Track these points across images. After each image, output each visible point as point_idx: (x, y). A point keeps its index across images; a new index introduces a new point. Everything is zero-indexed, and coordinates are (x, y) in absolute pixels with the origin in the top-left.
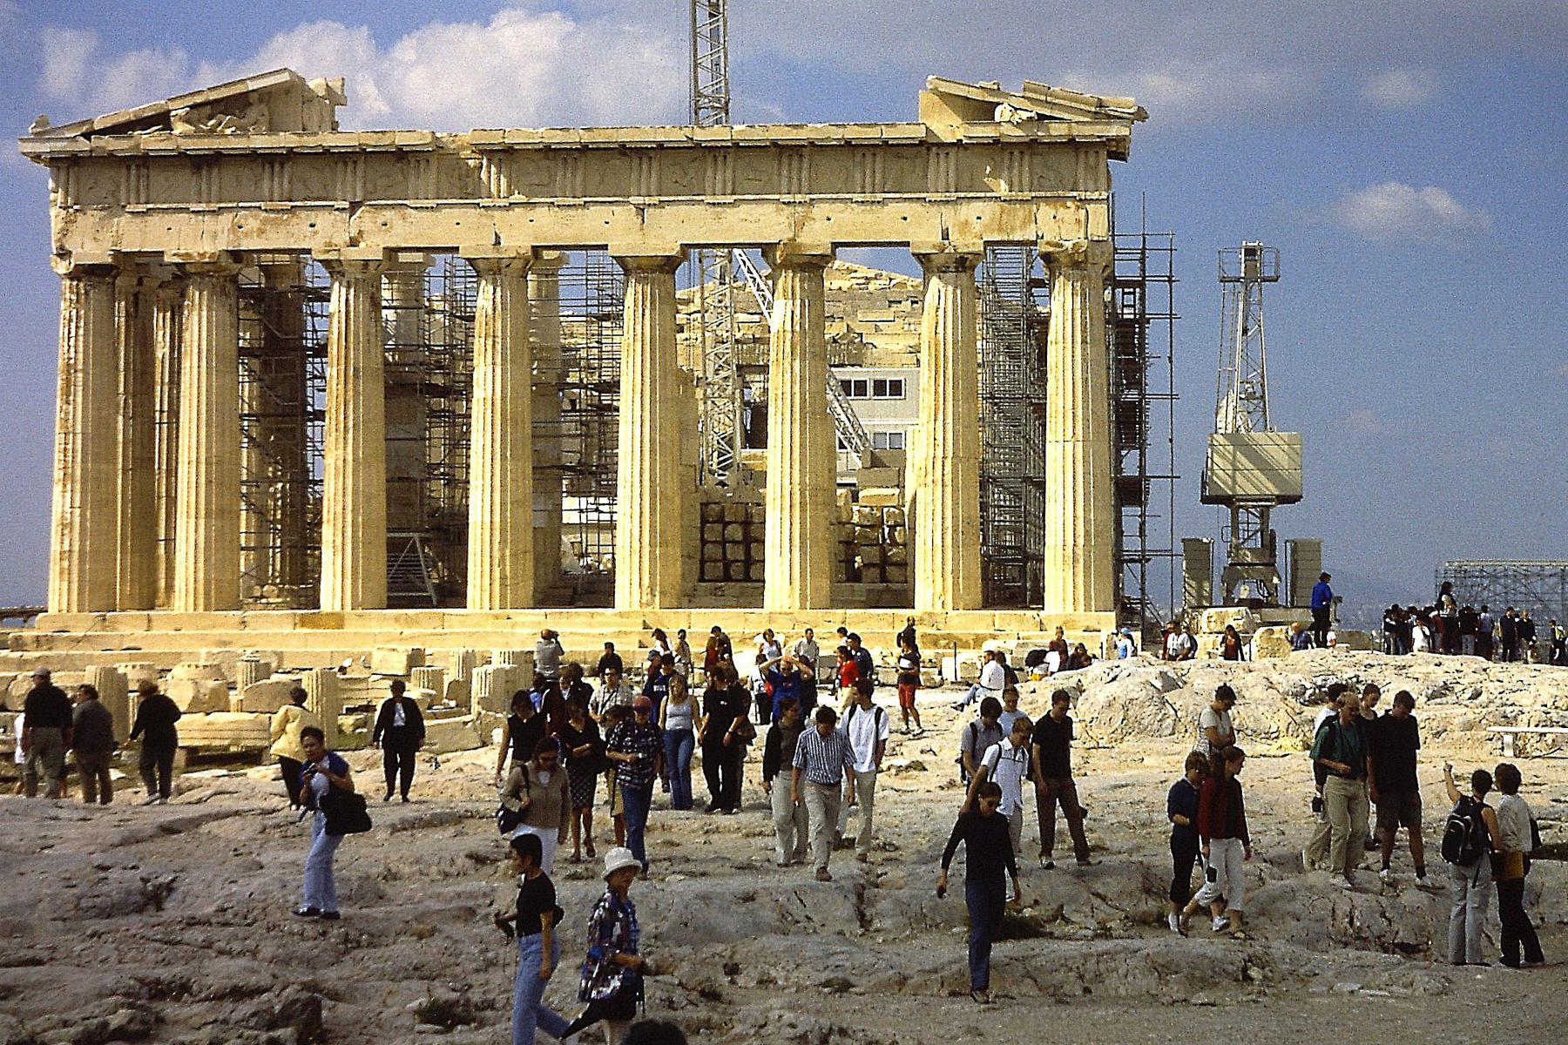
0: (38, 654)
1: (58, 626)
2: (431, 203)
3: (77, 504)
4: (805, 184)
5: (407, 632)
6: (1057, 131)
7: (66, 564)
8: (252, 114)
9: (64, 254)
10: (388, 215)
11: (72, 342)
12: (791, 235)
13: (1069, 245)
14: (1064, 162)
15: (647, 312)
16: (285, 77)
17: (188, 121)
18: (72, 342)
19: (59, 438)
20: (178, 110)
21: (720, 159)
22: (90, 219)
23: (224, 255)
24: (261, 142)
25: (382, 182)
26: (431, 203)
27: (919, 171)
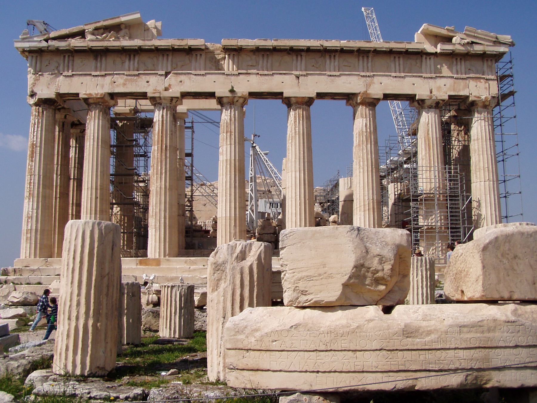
0: (15, 277)
1: (25, 264)
2: (203, 72)
3: (35, 207)
4: (370, 68)
5: (192, 267)
6: (478, 48)
7: (29, 235)
8: (122, 33)
9: (33, 95)
10: (182, 77)
11: (35, 134)
12: (365, 90)
13: (483, 97)
14: (478, 64)
15: (301, 122)
16: (138, 16)
17: (93, 34)
18: (35, 134)
19: (27, 178)
20: (89, 28)
21: (332, 57)
22: (47, 77)
23: (107, 95)
24: (126, 43)
25: (180, 64)
26: (203, 72)
27: (418, 64)
